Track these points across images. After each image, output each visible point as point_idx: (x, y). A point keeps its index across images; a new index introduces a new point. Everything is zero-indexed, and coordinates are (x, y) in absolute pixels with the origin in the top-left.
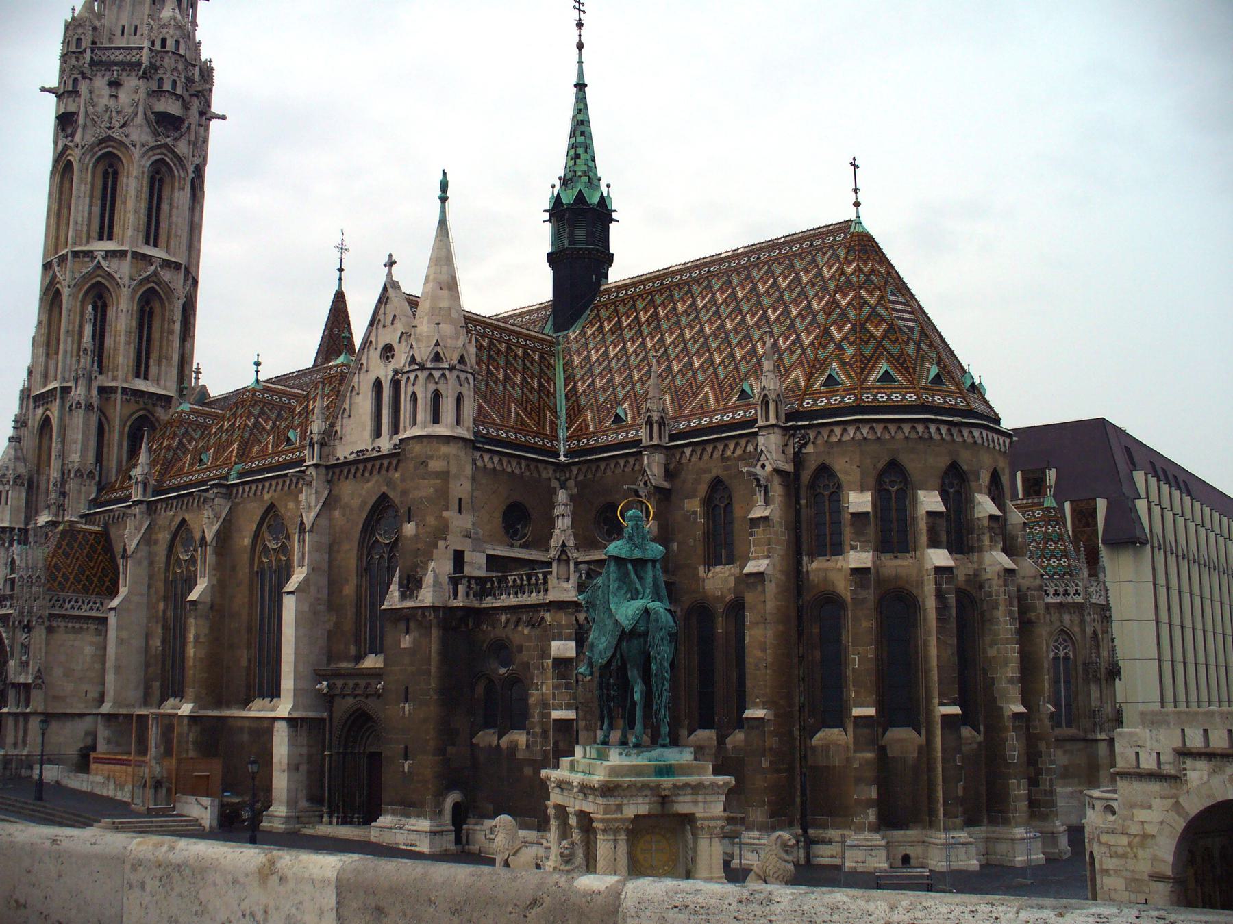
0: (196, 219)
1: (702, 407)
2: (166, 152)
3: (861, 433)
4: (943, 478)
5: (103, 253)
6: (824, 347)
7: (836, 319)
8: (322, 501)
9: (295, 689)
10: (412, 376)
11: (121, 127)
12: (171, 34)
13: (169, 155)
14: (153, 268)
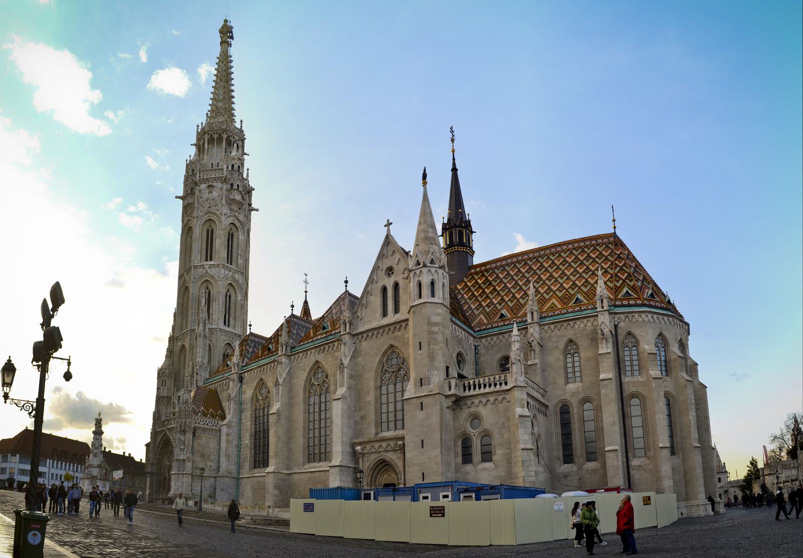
2: (235, 219)
8: (352, 352)
9: (342, 451)
13: (237, 221)
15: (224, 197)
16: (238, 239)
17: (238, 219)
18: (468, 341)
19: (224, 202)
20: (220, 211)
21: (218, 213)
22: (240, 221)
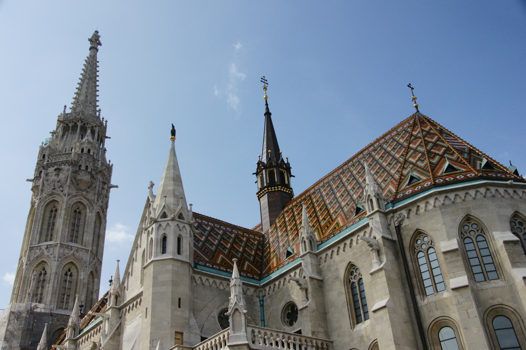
1: (335, 228)
6: (406, 168)
7: (411, 155)
10: (150, 229)
11: (59, 188)
13: (84, 200)
14: (72, 252)
16: (86, 216)
17: (85, 198)
21: (61, 194)
22: (88, 200)
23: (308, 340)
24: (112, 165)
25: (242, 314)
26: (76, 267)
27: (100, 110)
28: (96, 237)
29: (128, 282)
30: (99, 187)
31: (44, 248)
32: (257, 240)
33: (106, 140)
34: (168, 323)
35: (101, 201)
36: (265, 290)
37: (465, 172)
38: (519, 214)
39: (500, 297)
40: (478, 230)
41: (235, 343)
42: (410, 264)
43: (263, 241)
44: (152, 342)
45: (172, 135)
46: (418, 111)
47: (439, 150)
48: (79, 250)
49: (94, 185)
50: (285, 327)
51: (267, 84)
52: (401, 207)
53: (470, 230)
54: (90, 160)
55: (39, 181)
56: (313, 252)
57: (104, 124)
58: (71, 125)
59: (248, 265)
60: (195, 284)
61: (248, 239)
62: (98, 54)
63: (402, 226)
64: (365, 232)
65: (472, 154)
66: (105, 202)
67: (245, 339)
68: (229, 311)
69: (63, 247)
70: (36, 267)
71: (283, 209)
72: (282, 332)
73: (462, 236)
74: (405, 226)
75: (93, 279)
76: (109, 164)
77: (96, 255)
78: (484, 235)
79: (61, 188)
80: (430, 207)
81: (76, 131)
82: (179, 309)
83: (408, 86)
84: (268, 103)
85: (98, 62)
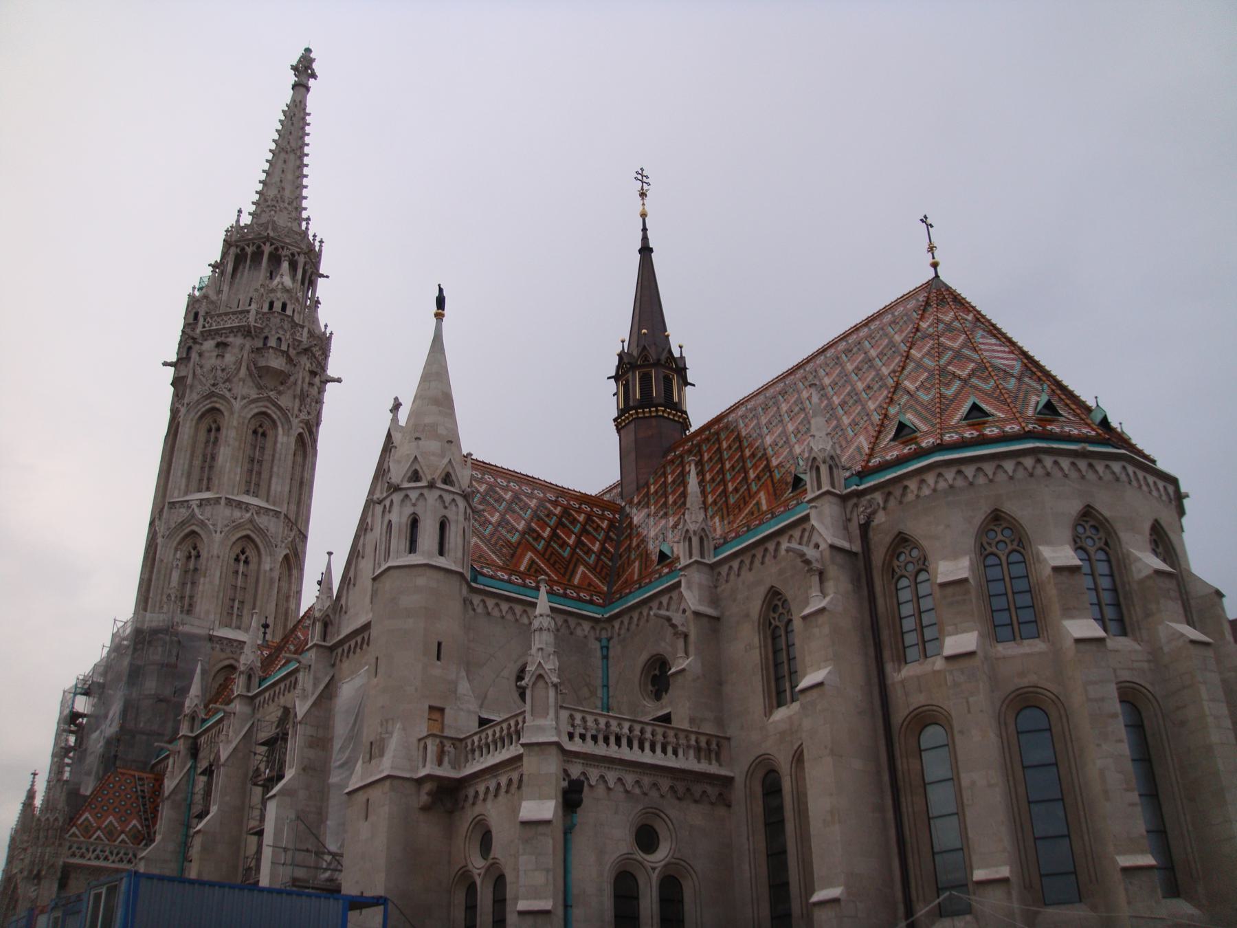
0: (306, 475)
1: (753, 514)
2: (270, 405)
3: (946, 480)
4: (1075, 527)
5: (198, 502)
8: (322, 687)
10: (387, 503)
11: (224, 383)
12: (280, 297)
13: (273, 408)
14: (248, 515)
15: (244, 364)
16: (275, 443)
18: (571, 633)
19: (243, 371)
20: (234, 391)
21: (228, 395)
22: (280, 408)
23: (682, 735)
24: (331, 334)
25: (550, 685)
26: (257, 547)
27: (308, 219)
28: (296, 485)
29: (347, 598)
30: (303, 382)
31: (194, 505)
32: (609, 519)
33: (320, 280)
34: (416, 690)
35: (306, 411)
36: (613, 627)
37: (1004, 420)
38: (1094, 512)
39: (1035, 673)
40: (1012, 541)
41: (534, 740)
42: (880, 601)
43: (620, 522)
44: (385, 723)
45: (438, 308)
46: (937, 276)
47: (963, 370)
48: (262, 511)
49: (292, 379)
50: (645, 703)
51: (648, 184)
52: (874, 485)
53: (997, 539)
54: (286, 327)
55: (186, 366)
56: (706, 561)
57: (317, 249)
58: (249, 250)
59: (583, 573)
60: (471, 613)
61: (589, 518)
62: (310, 97)
63: (874, 524)
64: (804, 530)
65: (1026, 380)
66: (314, 413)
67: (554, 732)
68: (527, 679)
69: (232, 506)
70: (180, 543)
71: (665, 455)
72: (630, 720)
73: (983, 550)
74: (878, 525)
75: (290, 569)
76: (325, 333)
77: (296, 524)
78: (1022, 550)
79: (227, 383)
80: (926, 491)
81: (260, 263)
82: (439, 663)
83: (922, 220)
84: (647, 227)
85: (309, 114)
